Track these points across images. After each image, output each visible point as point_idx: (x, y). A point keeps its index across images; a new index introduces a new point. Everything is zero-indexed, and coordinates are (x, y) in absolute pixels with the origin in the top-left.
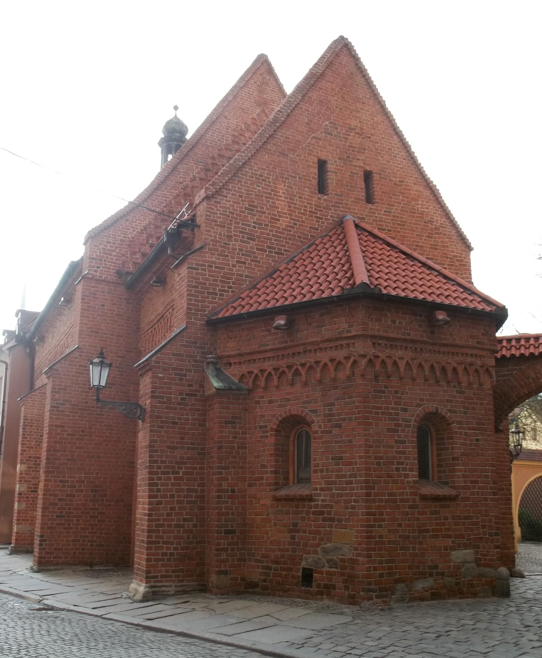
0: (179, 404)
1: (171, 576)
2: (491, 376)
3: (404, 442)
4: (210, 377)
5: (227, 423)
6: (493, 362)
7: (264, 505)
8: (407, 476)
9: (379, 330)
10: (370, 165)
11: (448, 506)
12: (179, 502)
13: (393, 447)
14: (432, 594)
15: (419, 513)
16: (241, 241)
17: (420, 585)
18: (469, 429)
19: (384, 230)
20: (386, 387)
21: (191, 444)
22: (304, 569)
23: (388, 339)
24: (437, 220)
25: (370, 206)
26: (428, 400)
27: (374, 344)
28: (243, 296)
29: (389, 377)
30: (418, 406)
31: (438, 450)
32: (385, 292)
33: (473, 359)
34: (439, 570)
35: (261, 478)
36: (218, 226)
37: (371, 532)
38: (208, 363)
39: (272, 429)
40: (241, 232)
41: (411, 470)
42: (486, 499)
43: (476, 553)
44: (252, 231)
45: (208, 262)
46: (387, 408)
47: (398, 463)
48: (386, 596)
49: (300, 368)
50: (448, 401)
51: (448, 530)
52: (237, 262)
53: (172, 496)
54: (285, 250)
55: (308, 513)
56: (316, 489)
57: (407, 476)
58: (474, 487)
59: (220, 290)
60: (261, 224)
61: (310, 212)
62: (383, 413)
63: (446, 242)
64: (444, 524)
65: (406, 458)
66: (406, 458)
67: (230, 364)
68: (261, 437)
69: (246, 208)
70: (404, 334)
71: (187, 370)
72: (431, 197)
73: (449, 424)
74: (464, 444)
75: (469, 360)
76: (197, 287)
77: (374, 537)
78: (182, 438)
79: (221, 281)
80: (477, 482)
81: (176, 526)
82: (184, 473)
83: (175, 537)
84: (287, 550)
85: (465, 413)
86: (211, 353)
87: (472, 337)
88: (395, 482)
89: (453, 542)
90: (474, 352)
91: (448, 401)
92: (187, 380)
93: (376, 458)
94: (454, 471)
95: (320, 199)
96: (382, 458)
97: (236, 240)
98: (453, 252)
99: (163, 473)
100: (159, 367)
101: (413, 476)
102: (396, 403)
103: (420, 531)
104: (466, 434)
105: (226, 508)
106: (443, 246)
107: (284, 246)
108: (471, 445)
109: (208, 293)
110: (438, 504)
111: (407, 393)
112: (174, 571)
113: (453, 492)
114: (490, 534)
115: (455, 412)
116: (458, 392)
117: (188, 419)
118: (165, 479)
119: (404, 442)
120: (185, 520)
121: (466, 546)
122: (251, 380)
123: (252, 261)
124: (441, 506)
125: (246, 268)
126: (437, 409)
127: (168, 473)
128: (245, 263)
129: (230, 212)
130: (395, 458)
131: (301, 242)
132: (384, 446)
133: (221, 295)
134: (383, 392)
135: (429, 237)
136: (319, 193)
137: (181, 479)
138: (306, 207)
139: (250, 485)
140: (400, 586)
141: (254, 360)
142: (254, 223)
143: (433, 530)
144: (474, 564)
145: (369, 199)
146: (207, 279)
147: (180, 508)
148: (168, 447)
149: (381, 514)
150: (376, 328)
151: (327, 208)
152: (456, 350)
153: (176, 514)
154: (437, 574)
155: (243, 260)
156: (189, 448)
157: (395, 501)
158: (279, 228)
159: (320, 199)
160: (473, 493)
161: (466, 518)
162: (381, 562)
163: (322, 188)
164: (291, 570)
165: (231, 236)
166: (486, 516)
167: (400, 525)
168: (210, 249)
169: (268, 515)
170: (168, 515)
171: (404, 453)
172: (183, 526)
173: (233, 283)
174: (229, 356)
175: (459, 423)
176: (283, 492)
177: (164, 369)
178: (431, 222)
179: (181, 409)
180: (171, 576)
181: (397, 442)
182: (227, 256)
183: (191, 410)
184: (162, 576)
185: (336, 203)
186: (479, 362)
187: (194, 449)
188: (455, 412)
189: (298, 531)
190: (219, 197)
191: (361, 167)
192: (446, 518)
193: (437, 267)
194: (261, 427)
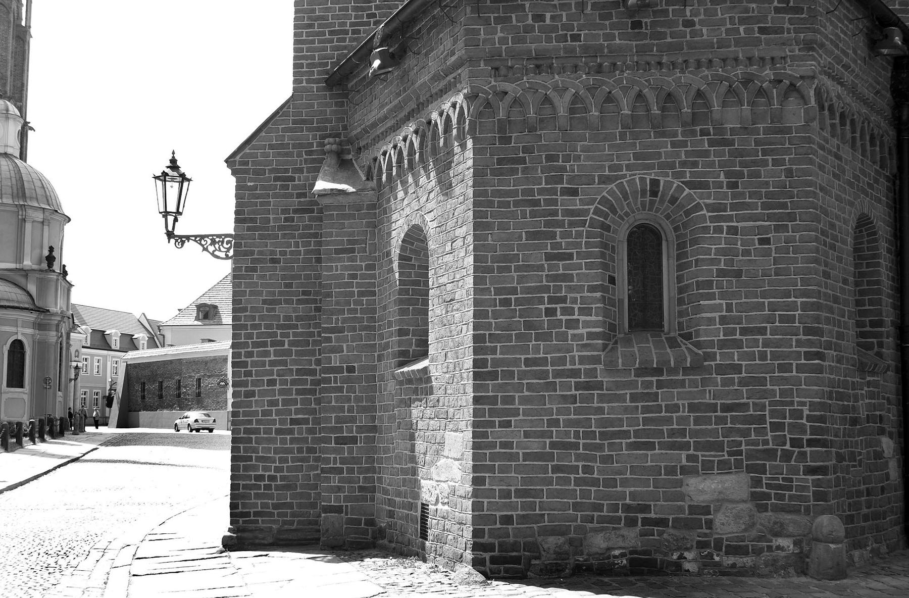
0: (281, 228)
3: (570, 257)
5: (338, 252)
9: (503, 41)
11: (682, 384)
12: (282, 392)
13: (541, 268)
14: (632, 561)
15: (601, 398)
18: (740, 219)
20: (526, 150)
21: (304, 293)
29: (532, 129)
30: (604, 180)
34: (653, 515)
41: (582, 311)
43: (757, 482)
47: (551, 300)
50: (683, 164)
51: (682, 433)
53: (272, 382)
59: (352, 24)
62: (517, 204)
64: (669, 421)
66: (570, 289)
71: (296, 170)
76: (310, 26)
77: (493, 445)
80: (762, 331)
82: (292, 344)
85: (734, 185)
87: (742, 21)
88: (546, 337)
89: (689, 458)
91: (683, 164)
92: (295, 187)
93: (498, 291)
94: (699, 309)
96: (514, 291)
99: (256, 345)
101: (587, 324)
104: (733, 231)
105: (337, 399)
108: (747, 253)
109: (332, 33)
114: (795, 443)
115: (704, 185)
116: (712, 143)
117: (299, 253)
119: (570, 257)
120: (293, 422)
121: (724, 467)
124: (660, 385)
127: (264, 344)
130: (547, 289)
132: (518, 269)
133: (354, 32)
137: (288, 353)
147: (286, 402)
149: (509, 400)
153: (278, 413)
154: (646, 522)
161: (727, 408)
162: (506, 494)
166: (782, 403)
167: (555, 423)
170: (264, 413)
171: (567, 278)
177: (256, 173)
179: (284, 236)
181: (549, 257)
186: (768, 73)
192: (675, 408)
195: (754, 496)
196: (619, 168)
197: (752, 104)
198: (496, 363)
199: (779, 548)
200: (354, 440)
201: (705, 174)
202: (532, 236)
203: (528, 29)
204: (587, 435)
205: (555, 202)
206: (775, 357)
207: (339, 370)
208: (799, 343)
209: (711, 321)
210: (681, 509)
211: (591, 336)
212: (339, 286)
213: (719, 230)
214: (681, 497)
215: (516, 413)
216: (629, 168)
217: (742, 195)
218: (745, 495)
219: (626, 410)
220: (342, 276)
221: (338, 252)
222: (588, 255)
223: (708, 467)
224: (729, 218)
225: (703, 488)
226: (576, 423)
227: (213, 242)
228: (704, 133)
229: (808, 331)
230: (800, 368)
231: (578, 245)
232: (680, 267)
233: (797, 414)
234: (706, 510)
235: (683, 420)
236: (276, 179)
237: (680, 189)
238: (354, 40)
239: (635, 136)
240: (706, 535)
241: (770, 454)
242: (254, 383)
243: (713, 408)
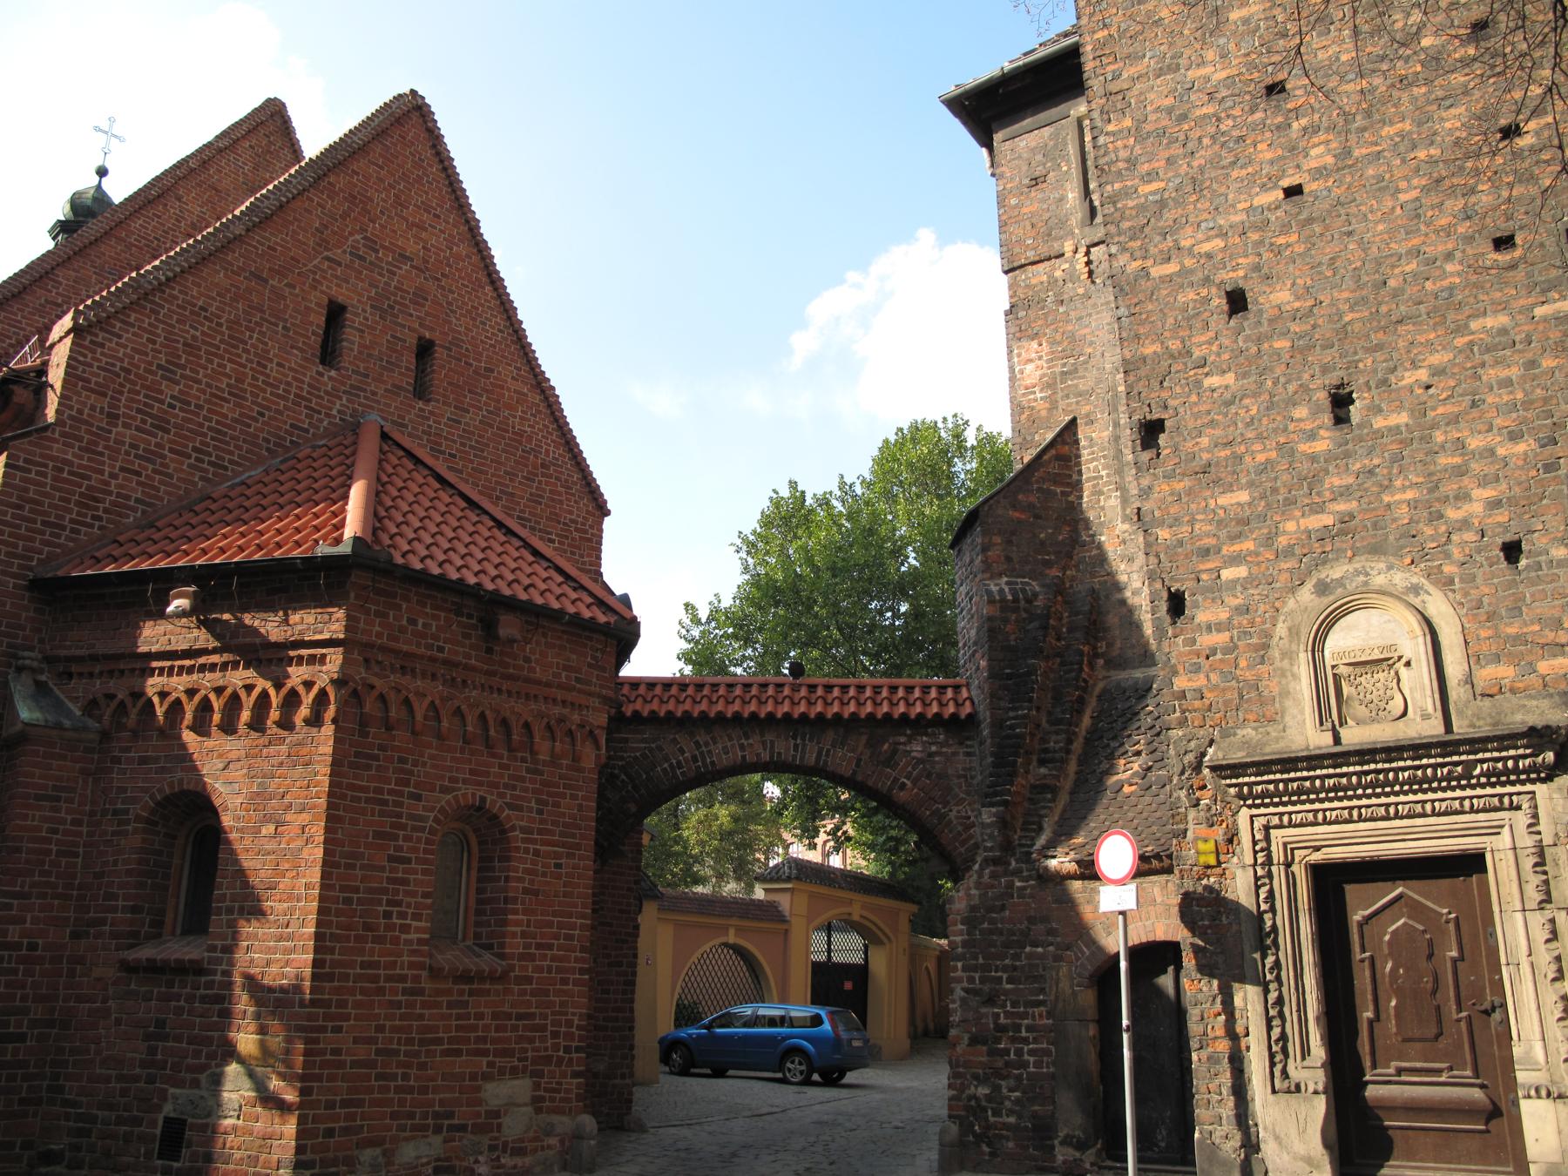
2: (598, 748)
3: (409, 861)
4: (16, 697)
6: (603, 719)
7: (99, 979)
8: (405, 929)
9: (379, 635)
10: (431, 329)
13: (383, 869)
15: (424, 1005)
16: (138, 429)
19: (443, 453)
20: (382, 748)
22: (167, 1120)
24: (547, 451)
25: (421, 404)
26: (465, 781)
27: (366, 660)
28: (121, 538)
29: (389, 728)
30: (445, 790)
31: (479, 880)
32: (400, 561)
33: (566, 711)
34: (456, 1122)
35: (103, 922)
36: (92, 391)
37: (316, 1041)
38: (20, 670)
39: (138, 818)
40: (139, 411)
41: (417, 917)
43: (537, 1086)
44: (166, 412)
45: (52, 458)
46: (379, 791)
47: (389, 903)
49: (212, 697)
50: (506, 786)
51: (484, 1040)
52: (122, 469)
54: (231, 462)
55: (190, 999)
56: (213, 949)
58: (544, 957)
59: (72, 521)
60: (189, 403)
61: (297, 395)
62: (368, 800)
63: (560, 494)
65: (407, 893)
66: (407, 893)
67: (70, 676)
68: (114, 833)
69: (160, 367)
70: (429, 647)
75: (557, 710)
77: (322, 1052)
79: (78, 504)
80: (550, 947)
84: (136, 1079)
85: (540, 812)
86: (31, 649)
87: (565, 668)
88: (379, 940)
89: (490, 1065)
90: (570, 697)
91: (506, 786)
93: (343, 889)
94: (505, 923)
95: (322, 375)
96: (357, 890)
97: (126, 425)
98: (571, 513)
101: (418, 930)
102: (399, 782)
103: (422, 1042)
104: (537, 853)
106: (553, 500)
107: (232, 453)
108: (544, 874)
109: (44, 523)
110: (466, 987)
111: (424, 764)
113: (500, 966)
114: (567, 1050)
115: (519, 808)
116: (528, 771)
119: (409, 861)
121: (514, 1072)
122: (109, 712)
123: (154, 471)
125: (139, 483)
128: (138, 474)
129: (122, 368)
130: (385, 891)
131: (268, 449)
132: (363, 867)
133: (73, 531)
134: (376, 758)
136: (323, 362)
138: (288, 384)
139: (75, 936)
141: (122, 672)
142: (172, 397)
144: (529, 1109)
145: (421, 390)
146: (46, 495)
149: (342, 1004)
151: (334, 395)
154: (451, 1128)
155: (136, 467)
157: (375, 979)
158: (226, 416)
159: (322, 375)
160: (540, 969)
161: (520, 1017)
162: (330, 1105)
163: (328, 353)
164: (137, 1122)
165: (117, 417)
167: (380, 1029)
168: (64, 435)
169: (105, 1001)
171: (404, 882)
173: (106, 511)
174: (69, 659)
175: (524, 830)
176: (145, 953)
178: (537, 452)
181: (391, 859)
182: (102, 454)
185: (352, 386)
186: (576, 717)
189: (165, 1038)
190: (101, 334)
191: (414, 330)
192: (480, 1016)
193: (523, 533)
194: (115, 812)
195: (536, 1100)
196: (455, 780)
199: (549, 1147)
200: (22, 1038)
202: (377, 835)
203: (402, 630)
204: (409, 1041)
205: (401, 805)
206: (559, 970)
209: (514, 935)
210: (478, 1114)
211: (420, 941)
213: (527, 851)
214: (479, 1102)
215: (347, 1018)
218: (527, 1099)
221: (38, 798)
222: (426, 861)
223: (502, 1072)
224: (534, 841)
225: (496, 1092)
226: (394, 1029)
231: (415, 850)
233: (569, 1023)
234: (496, 1114)
235: (486, 1028)
237: (501, 809)
238: (72, 540)
240: (496, 1139)
241: (548, 1060)
243: (509, 1016)
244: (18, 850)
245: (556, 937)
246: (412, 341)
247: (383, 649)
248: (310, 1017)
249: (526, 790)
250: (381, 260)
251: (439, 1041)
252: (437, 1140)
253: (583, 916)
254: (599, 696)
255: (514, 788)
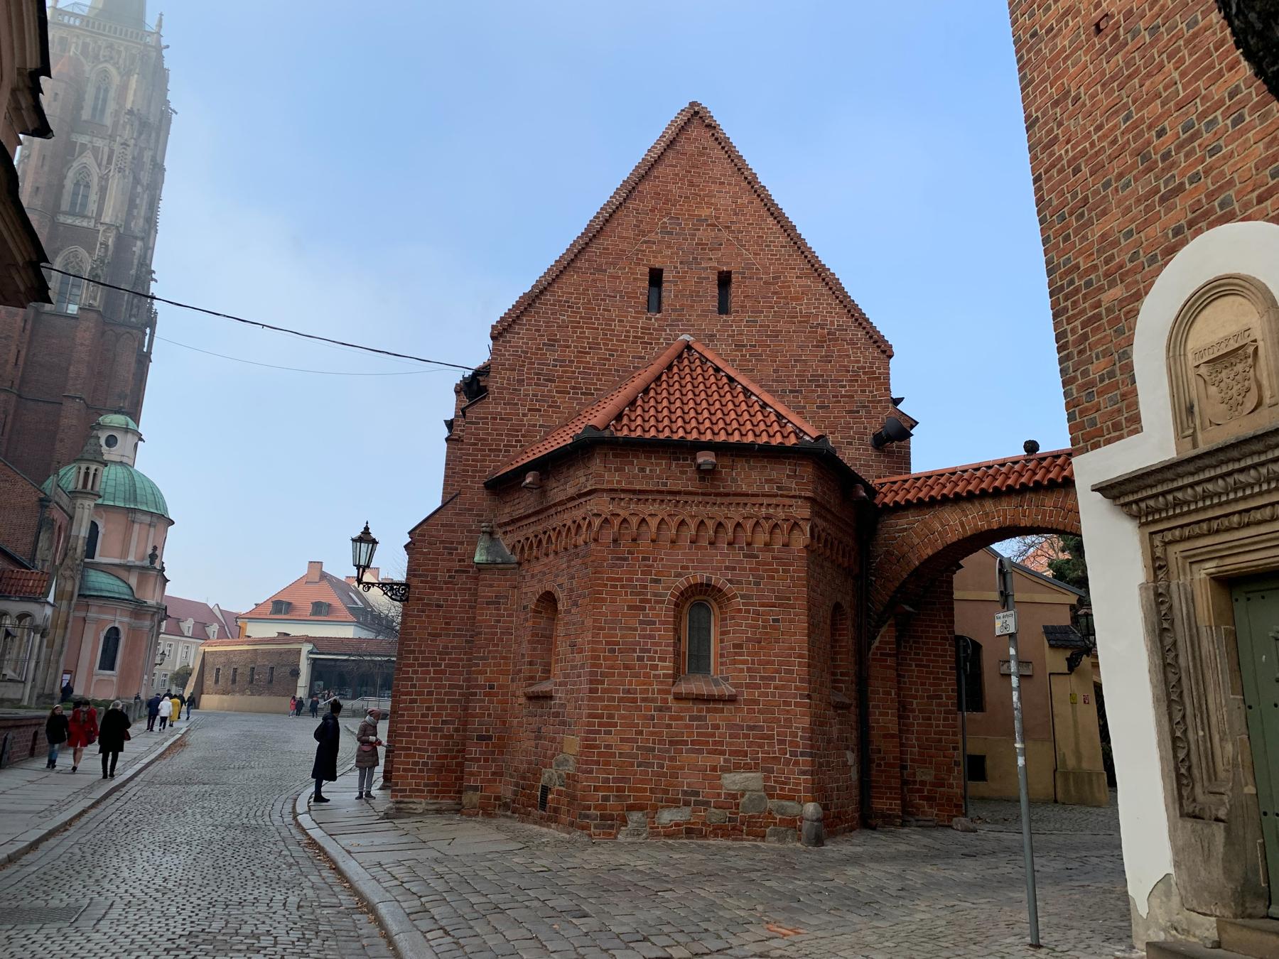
0: (446, 583)
1: (423, 791)
8: (655, 667)
9: (618, 482)
10: (728, 264)
12: (437, 701)
15: (671, 718)
17: (667, 817)
23: (634, 492)
24: (832, 322)
25: (724, 317)
30: (678, 575)
33: (771, 511)
41: (661, 659)
42: (787, 704)
43: (767, 779)
45: (491, 413)
46: (631, 580)
47: (642, 651)
48: (611, 827)
51: (721, 743)
53: (430, 693)
54: (596, 390)
57: (655, 667)
58: (767, 686)
62: (622, 587)
64: (713, 735)
72: (825, 290)
73: (729, 599)
74: (751, 626)
77: (598, 747)
78: (447, 624)
79: (507, 435)
81: (433, 729)
83: (430, 744)
87: (767, 481)
88: (637, 675)
89: (725, 761)
91: (727, 568)
93: (608, 643)
98: (858, 362)
99: (421, 665)
100: (424, 541)
101: (663, 668)
102: (643, 573)
103: (671, 743)
105: (481, 708)
112: (426, 785)
114: (793, 754)
115: (739, 582)
116: (745, 556)
118: (423, 673)
120: (444, 722)
121: (748, 768)
124: (708, 711)
126: (709, 579)
127: (427, 665)
132: (621, 629)
134: (625, 559)
135: (817, 346)
137: (443, 672)
138: (628, 332)
140: (635, 816)
143: (693, 742)
145: (723, 308)
146: (488, 434)
147: (439, 708)
148: (429, 634)
149: (611, 716)
150: (613, 479)
152: (745, 500)
154: (697, 803)
156: (455, 635)
160: (766, 695)
161: (751, 728)
166: (784, 727)
167: (641, 733)
170: (423, 716)
171: (651, 637)
172: (441, 730)
173: (523, 436)
180: (423, 791)
181: (641, 622)
183: (460, 589)
184: (411, 790)
186: (781, 514)
187: (460, 636)
188: (739, 582)
191: (714, 268)
192: (717, 727)
195: (765, 788)
197: (771, 533)
198: (604, 691)
201: (740, 575)
202: (630, 608)
204: (661, 742)
207: (483, 687)
208: (797, 688)
209: (741, 670)
212: (488, 627)
213: (748, 611)
214: (721, 787)
216: (694, 568)
217: (763, 590)
219: (687, 726)
220: (489, 620)
224: (753, 605)
225: (733, 781)
226: (652, 733)
227: (392, 589)
228: (741, 549)
229: (802, 681)
230: (796, 704)
232: (723, 633)
234: (734, 797)
236: (445, 548)
239: (699, 548)
242: (418, 694)
244: (480, 633)
245: (778, 671)
246: (714, 277)
247: (623, 491)
248: (589, 724)
249: (745, 569)
250: (684, 229)
251: (686, 743)
252: (687, 810)
253: (801, 656)
254: (800, 497)
255: (734, 569)
